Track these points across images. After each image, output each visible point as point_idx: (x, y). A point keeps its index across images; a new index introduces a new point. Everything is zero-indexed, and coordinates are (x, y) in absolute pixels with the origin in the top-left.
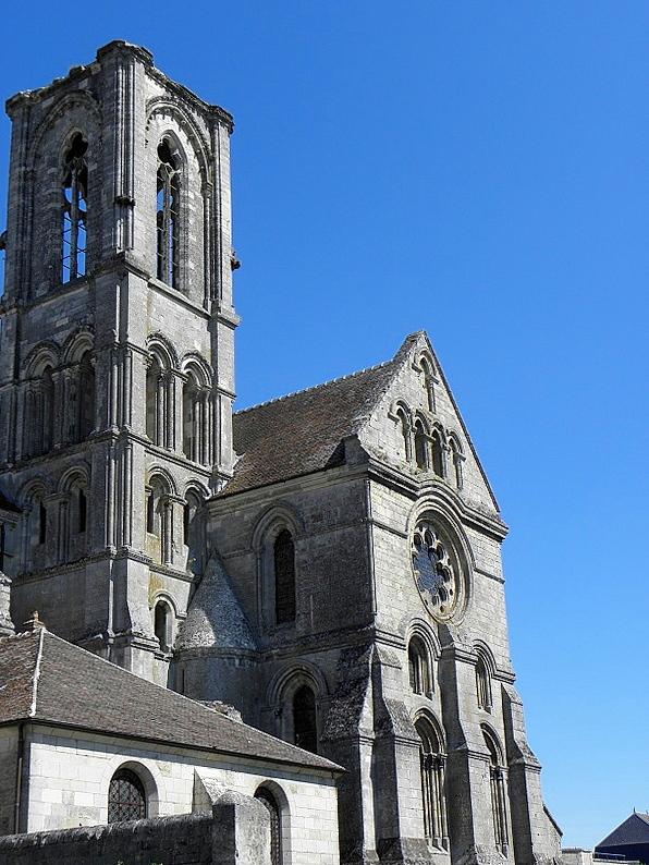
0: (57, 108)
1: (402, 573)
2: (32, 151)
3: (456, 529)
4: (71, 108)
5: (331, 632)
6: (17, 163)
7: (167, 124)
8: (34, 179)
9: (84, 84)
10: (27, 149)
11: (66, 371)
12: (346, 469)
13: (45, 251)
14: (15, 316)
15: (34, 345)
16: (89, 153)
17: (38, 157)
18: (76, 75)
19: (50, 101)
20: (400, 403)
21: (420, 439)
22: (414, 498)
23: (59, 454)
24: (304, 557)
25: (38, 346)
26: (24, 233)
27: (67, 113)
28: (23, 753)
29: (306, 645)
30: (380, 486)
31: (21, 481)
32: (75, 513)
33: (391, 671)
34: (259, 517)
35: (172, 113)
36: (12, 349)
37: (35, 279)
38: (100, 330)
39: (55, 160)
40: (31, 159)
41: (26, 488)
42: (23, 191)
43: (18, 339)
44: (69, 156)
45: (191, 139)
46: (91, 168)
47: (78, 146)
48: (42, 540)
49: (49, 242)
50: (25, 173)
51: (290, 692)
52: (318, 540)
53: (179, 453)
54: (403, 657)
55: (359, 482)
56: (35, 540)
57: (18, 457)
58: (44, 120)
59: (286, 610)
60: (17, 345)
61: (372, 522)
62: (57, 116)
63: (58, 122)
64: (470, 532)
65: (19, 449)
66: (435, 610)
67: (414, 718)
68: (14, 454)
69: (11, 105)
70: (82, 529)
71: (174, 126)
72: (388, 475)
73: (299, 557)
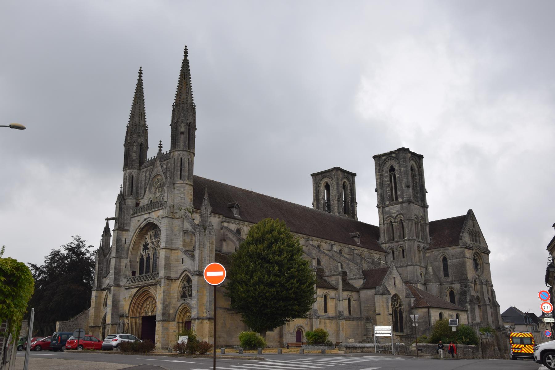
0: (387, 160)
1: (472, 267)
2: (381, 169)
3: (480, 254)
4: (390, 160)
5: (458, 280)
6: (378, 172)
7: (412, 162)
8: (382, 176)
9: (393, 155)
10: (380, 168)
11: (396, 223)
12: (459, 247)
13: (387, 193)
14: (382, 209)
15: (387, 216)
16: (396, 172)
17: (383, 171)
18: (392, 153)
19: (384, 158)
20: (469, 229)
21: (472, 235)
22: (472, 250)
23: (397, 242)
24: (450, 264)
25: (388, 217)
26: (381, 188)
27: (389, 161)
28: (429, 312)
29: (452, 282)
30: (467, 249)
31: (387, 246)
32: (401, 254)
33: (472, 289)
34: (439, 254)
35: (412, 159)
36: (382, 217)
37: (385, 200)
38: (405, 216)
39: (387, 172)
40: (381, 171)
41: (389, 248)
42: (380, 179)
43: (383, 214)
44: (390, 171)
45: (416, 164)
46: (397, 176)
47: (392, 169)
48: (394, 259)
49: (388, 192)
50: (380, 174)
51: (448, 292)
52: (453, 261)
53: (421, 240)
54: (473, 285)
55: (463, 249)
56: (392, 259)
57: (386, 241)
58: (383, 162)
59: (446, 274)
60: (383, 216)
61: (466, 258)
62: (387, 161)
63: (387, 162)
64: (483, 254)
65: (386, 239)
66: (477, 273)
67: (475, 297)
68: (385, 240)
69: (375, 157)
70: (404, 257)
71: (414, 163)
72: (468, 247)
73: (449, 264)
